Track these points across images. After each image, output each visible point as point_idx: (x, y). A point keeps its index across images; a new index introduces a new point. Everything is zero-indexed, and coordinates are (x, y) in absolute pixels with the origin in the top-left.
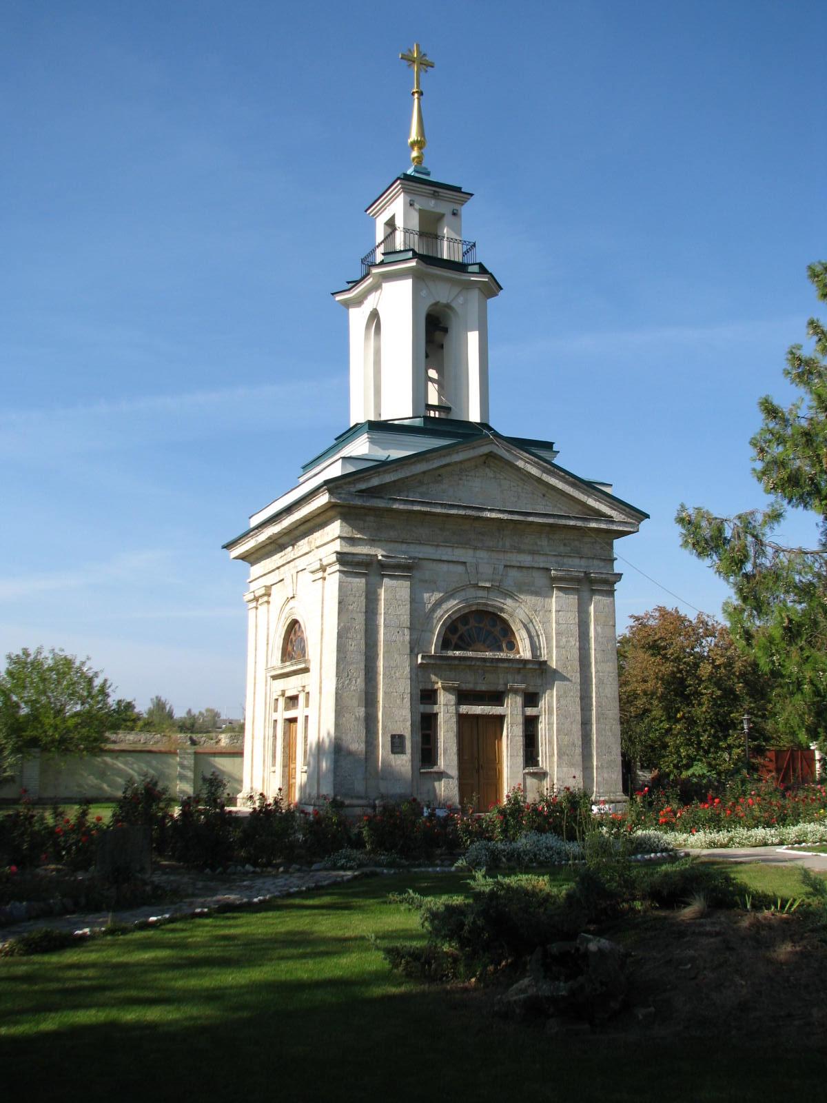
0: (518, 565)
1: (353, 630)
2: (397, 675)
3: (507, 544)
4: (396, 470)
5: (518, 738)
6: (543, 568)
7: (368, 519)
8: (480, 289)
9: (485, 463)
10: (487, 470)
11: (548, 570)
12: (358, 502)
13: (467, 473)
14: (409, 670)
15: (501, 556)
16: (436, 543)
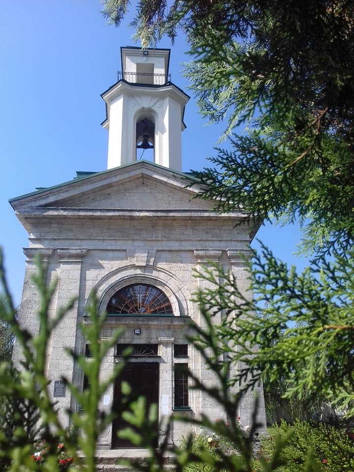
0: (168, 249)
1: (33, 302)
2: (65, 333)
3: (160, 235)
4: (68, 190)
5: (167, 382)
6: (189, 251)
7: (52, 226)
8: (170, 96)
9: (143, 183)
10: (146, 188)
11: (193, 251)
12: (38, 213)
13: (130, 192)
14: (75, 330)
15: (154, 243)
16: (102, 238)
